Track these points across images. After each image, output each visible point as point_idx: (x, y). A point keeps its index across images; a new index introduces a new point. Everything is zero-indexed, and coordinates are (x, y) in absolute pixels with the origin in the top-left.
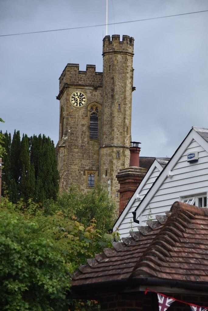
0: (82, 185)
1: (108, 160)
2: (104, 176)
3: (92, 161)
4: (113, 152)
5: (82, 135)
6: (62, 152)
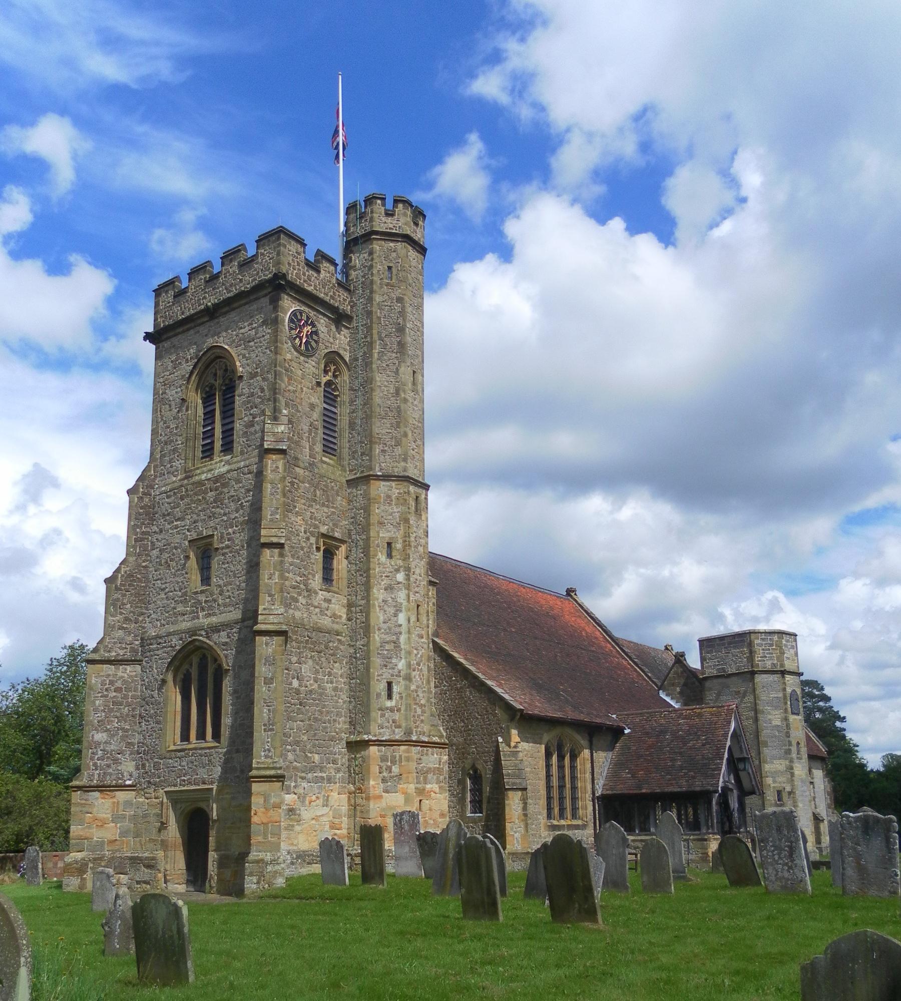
0: (314, 576)
1: (397, 515)
2: (382, 557)
3: (333, 513)
4: (409, 493)
5: (310, 432)
6: (277, 467)
